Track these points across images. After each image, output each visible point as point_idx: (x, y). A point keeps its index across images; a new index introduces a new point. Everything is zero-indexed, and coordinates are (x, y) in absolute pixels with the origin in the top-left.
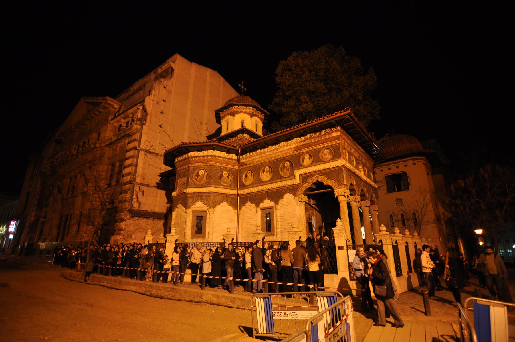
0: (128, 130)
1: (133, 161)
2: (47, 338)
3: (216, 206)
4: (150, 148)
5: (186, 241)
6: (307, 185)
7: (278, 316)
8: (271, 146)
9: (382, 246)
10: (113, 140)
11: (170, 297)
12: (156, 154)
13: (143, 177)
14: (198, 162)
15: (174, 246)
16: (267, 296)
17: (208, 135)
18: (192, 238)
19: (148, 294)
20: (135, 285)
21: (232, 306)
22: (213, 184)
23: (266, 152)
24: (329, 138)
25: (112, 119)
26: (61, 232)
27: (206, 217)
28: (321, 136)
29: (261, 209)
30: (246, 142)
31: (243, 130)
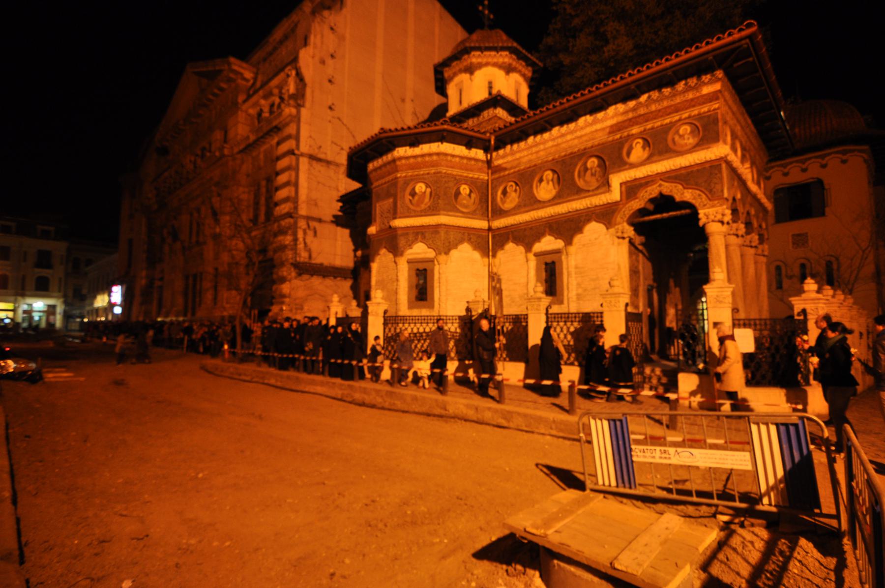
1: (290, 176)
2: (200, 475)
3: (449, 250)
4: (317, 151)
5: (401, 313)
6: (637, 204)
7: (645, 457)
8: (557, 128)
9: (805, 320)
11: (386, 405)
12: (328, 163)
14: (412, 167)
15: (382, 320)
16: (619, 416)
18: (410, 307)
19: (349, 399)
20: (322, 384)
21: (504, 423)
22: (444, 210)
23: (545, 142)
24: (692, 100)
29: (536, 255)
31: (496, 100)
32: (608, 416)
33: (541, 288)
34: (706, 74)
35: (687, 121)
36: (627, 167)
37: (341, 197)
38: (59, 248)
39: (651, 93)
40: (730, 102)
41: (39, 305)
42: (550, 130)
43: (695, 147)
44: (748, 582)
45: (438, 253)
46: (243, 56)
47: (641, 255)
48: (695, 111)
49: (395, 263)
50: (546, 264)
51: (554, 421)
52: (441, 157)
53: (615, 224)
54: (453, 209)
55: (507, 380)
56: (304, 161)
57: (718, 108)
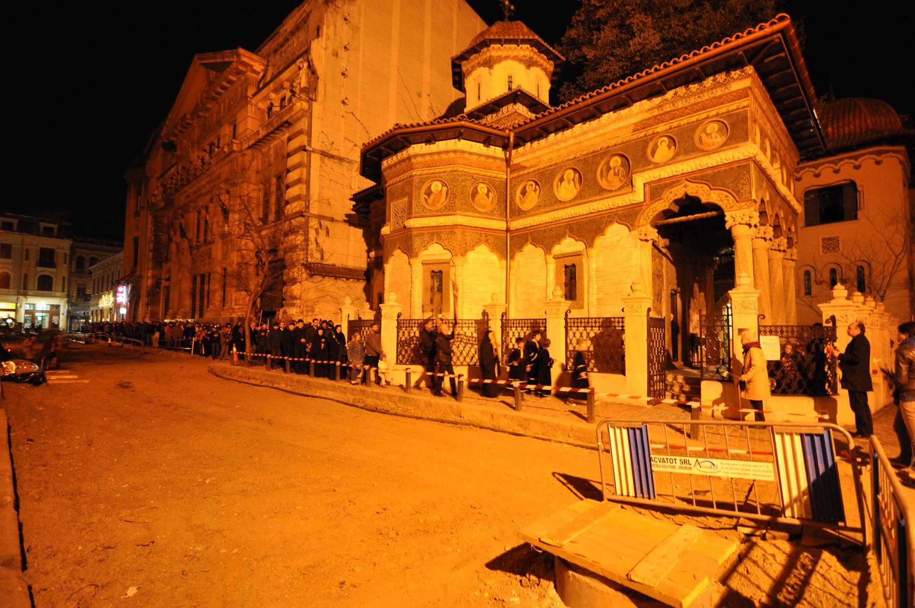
0: (287, 113)
1: (302, 172)
2: (208, 481)
3: (466, 251)
4: (329, 147)
5: (415, 317)
7: (665, 466)
8: (579, 125)
10: (261, 136)
11: (399, 411)
12: (341, 159)
16: (639, 425)
19: (362, 405)
20: (334, 389)
21: (522, 432)
22: (460, 210)
24: (720, 97)
25: (254, 95)
26: (198, 303)
27: (448, 273)
28: (702, 92)
31: (516, 96)
33: (560, 292)
34: (735, 70)
35: (715, 119)
36: (652, 166)
38: (62, 246)
39: (678, 89)
40: (760, 99)
41: (42, 304)
42: (572, 127)
43: (722, 146)
44: (768, 595)
46: (253, 47)
47: (664, 258)
48: (723, 109)
50: (566, 267)
52: (458, 154)
54: (470, 209)
56: (315, 158)
57: (748, 106)
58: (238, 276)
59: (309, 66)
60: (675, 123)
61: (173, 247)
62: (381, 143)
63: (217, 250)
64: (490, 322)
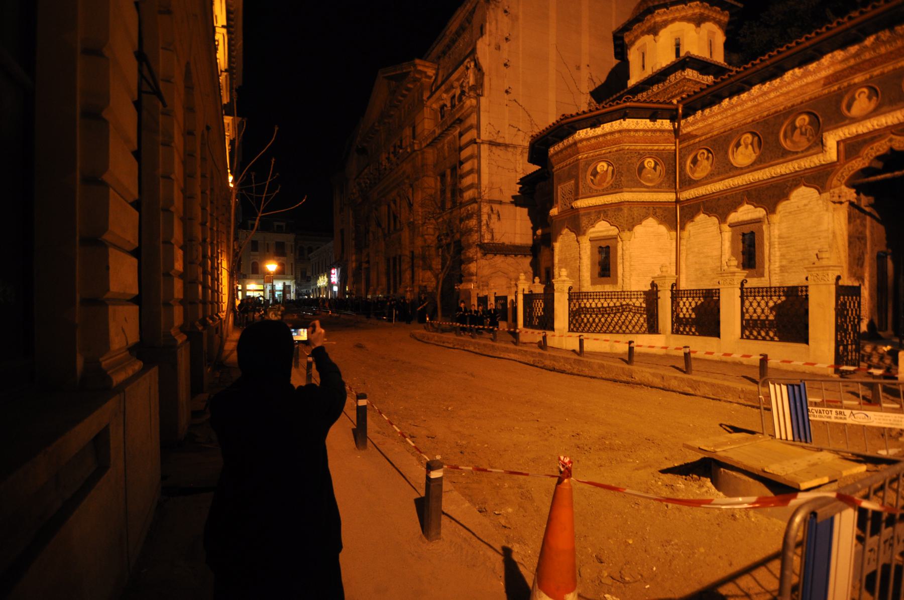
0: (458, 111)
1: (473, 164)
3: (633, 226)
4: (496, 136)
5: (584, 290)
6: (858, 164)
7: (821, 417)
8: (757, 86)
10: (437, 135)
11: (575, 371)
13: (491, 189)
14: (594, 148)
15: (567, 296)
16: (798, 382)
17: (593, 88)
18: (593, 283)
20: (515, 352)
21: (691, 391)
22: (627, 187)
25: (429, 98)
26: (392, 282)
30: (691, 88)
31: (684, 62)
32: (787, 382)
36: (847, 122)
37: (521, 179)
38: (289, 239)
39: (880, 34)
42: (749, 90)
45: (621, 229)
47: (868, 218)
49: (578, 242)
50: (744, 235)
51: (743, 391)
53: (831, 188)
54: (636, 185)
55: (695, 352)
56: (484, 148)
58: (423, 258)
59: (476, 65)
60: (877, 71)
61: (371, 235)
62: (549, 134)
63: (406, 235)
64: (660, 294)
